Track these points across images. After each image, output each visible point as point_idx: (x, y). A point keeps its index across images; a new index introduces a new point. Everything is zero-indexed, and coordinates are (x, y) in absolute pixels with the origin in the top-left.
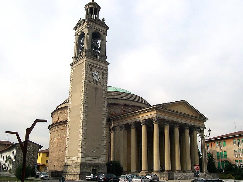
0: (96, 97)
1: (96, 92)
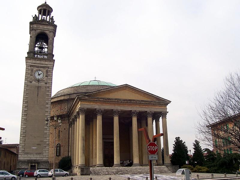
0: (38, 95)
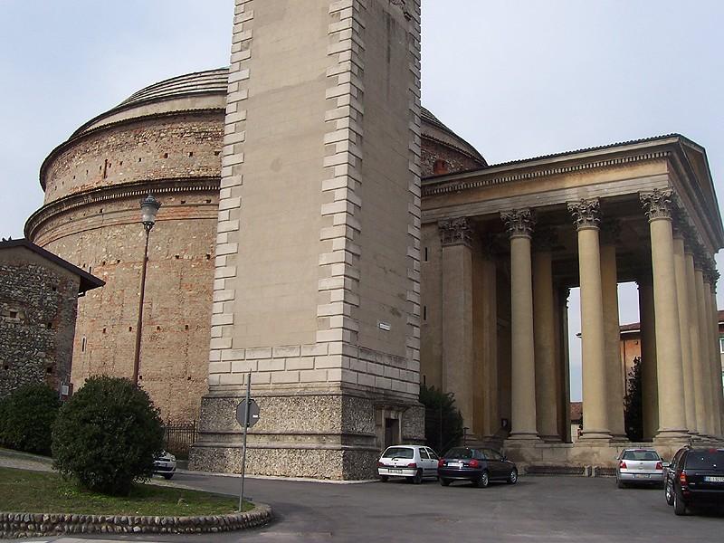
1: (389, 36)
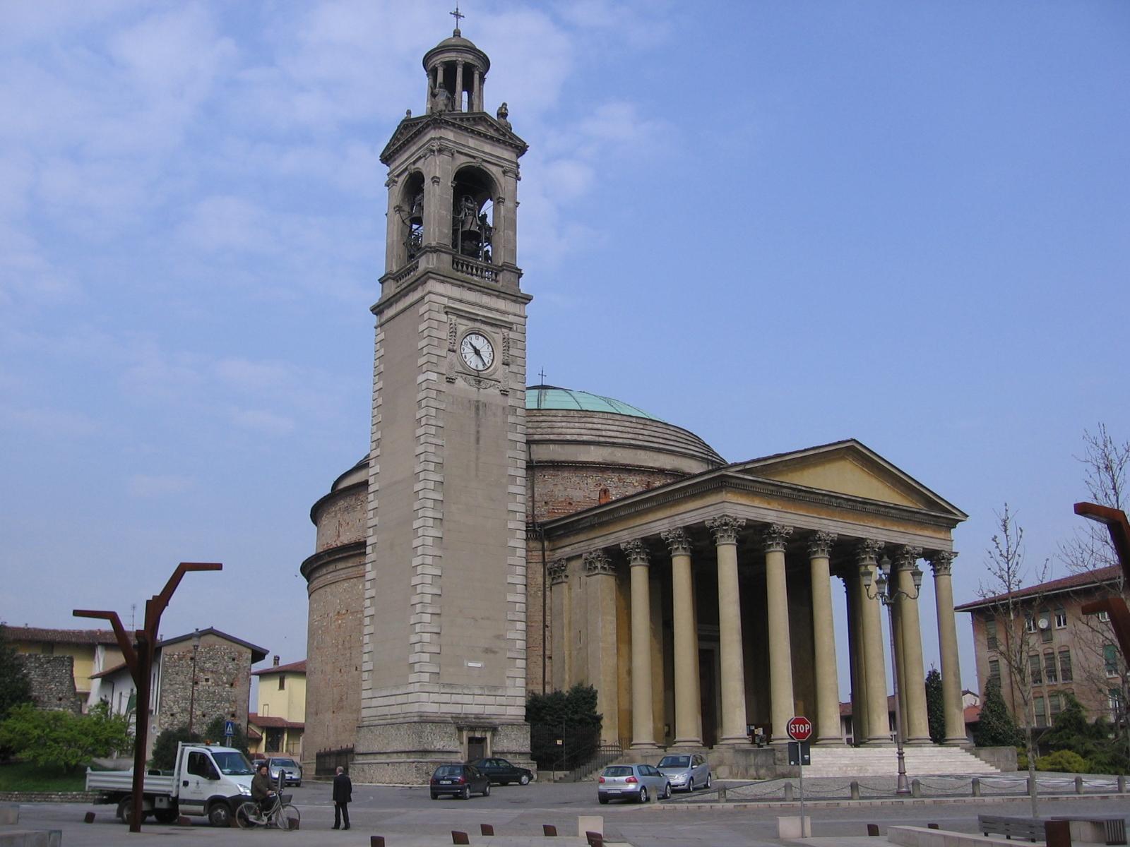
0: (478, 440)
